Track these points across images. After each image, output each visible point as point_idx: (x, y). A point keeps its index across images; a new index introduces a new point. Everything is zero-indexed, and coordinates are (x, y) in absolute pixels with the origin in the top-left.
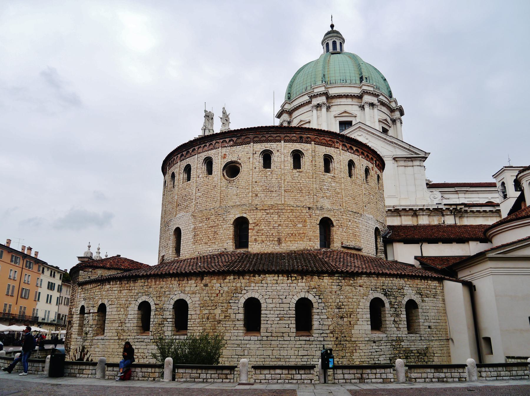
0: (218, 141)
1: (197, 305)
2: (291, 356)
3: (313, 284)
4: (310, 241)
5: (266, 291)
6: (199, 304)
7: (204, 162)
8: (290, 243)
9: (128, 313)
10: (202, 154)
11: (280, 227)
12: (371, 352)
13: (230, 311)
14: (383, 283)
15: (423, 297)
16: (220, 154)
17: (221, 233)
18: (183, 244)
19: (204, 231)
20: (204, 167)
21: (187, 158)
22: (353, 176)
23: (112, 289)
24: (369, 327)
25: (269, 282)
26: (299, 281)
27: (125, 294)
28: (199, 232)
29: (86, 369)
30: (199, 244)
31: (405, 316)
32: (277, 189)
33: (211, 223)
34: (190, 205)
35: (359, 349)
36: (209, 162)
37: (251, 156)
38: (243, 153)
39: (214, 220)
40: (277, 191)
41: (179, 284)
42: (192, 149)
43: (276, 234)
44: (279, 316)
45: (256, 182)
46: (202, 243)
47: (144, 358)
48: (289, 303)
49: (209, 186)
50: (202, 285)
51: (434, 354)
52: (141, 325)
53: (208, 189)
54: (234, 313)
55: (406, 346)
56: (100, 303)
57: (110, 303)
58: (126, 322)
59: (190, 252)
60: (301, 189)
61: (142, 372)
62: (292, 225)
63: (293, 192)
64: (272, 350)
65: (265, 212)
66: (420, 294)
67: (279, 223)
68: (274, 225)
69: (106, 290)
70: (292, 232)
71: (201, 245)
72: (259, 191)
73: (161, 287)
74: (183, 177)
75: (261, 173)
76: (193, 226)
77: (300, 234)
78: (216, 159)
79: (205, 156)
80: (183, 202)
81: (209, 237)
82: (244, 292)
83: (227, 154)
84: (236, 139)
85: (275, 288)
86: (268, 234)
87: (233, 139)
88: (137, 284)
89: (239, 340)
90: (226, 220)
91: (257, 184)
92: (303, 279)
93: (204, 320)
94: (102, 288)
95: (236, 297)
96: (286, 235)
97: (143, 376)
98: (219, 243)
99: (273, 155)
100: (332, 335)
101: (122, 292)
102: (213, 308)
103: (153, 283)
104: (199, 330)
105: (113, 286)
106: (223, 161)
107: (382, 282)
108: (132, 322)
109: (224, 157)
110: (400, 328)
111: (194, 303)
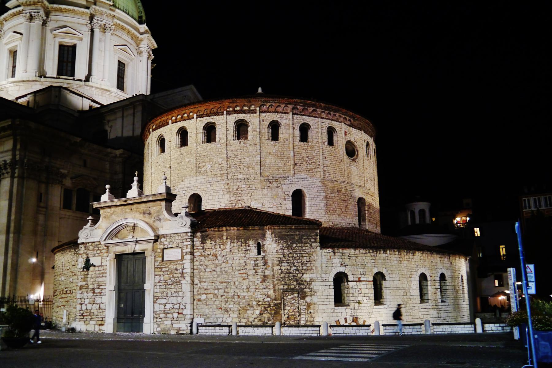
0: (341, 115)
10: (325, 120)
19: (336, 203)
27: (405, 265)
28: (331, 202)
30: (333, 215)
33: (342, 196)
38: (357, 137)
42: (312, 109)
46: (336, 214)
49: (336, 158)
57: (390, 272)
58: (411, 291)
73: (432, 262)
76: (324, 194)
80: (304, 163)
88: (415, 257)
103: (427, 258)
105: (391, 256)
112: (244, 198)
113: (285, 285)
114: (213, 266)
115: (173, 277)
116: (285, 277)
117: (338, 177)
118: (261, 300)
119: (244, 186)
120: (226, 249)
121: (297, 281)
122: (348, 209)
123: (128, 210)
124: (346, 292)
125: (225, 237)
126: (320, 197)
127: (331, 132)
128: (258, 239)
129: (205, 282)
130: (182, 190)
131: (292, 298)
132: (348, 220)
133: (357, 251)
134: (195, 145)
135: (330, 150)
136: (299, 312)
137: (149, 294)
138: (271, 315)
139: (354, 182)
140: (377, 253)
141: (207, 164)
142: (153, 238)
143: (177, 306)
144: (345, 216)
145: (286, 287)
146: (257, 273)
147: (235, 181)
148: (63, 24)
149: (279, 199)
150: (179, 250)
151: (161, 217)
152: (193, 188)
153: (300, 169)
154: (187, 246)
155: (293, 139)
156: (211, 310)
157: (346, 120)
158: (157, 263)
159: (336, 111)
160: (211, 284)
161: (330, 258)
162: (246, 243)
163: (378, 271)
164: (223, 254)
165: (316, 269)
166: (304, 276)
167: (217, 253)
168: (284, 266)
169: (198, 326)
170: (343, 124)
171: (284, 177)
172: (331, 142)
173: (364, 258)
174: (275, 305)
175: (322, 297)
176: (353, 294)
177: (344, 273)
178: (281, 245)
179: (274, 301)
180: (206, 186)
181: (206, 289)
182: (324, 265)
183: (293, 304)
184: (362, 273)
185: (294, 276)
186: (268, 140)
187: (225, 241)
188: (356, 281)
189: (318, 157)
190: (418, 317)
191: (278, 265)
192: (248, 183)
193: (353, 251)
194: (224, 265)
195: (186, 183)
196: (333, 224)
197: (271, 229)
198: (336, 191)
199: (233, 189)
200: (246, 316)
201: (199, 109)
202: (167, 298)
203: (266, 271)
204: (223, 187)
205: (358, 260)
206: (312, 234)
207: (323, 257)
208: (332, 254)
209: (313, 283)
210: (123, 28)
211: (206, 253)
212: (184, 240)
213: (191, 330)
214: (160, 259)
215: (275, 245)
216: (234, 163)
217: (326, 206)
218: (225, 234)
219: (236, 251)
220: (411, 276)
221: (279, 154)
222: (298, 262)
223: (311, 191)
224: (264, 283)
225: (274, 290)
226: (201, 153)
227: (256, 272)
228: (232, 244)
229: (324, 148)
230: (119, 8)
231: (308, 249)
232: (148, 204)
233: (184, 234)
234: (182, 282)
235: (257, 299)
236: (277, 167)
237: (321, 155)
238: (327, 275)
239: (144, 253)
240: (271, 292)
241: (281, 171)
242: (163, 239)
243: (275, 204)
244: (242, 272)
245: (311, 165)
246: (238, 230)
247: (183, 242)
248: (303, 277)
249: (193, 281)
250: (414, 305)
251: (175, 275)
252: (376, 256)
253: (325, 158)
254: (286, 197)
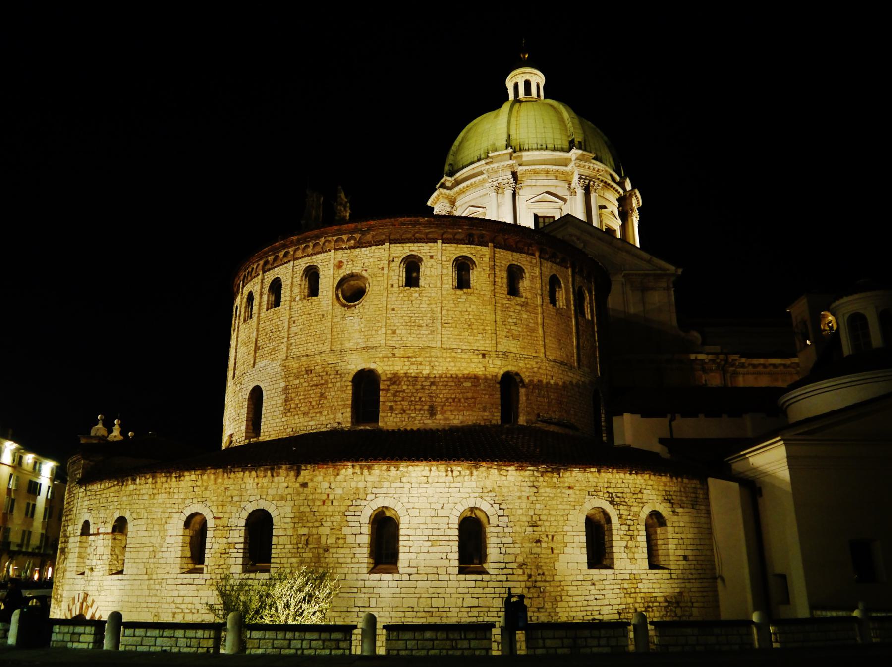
0: (330, 238)
1: (289, 520)
2: (450, 607)
3: (489, 484)
4: (484, 411)
5: (408, 495)
6: (291, 518)
7: (304, 274)
8: (450, 414)
9: (165, 534)
10: (300, 261)
11: (434, 388)
12: (588, 600)
13: (346, 531)
14: (607, 482)
15: (674, 506)
17: (331, 397)
18: (267, 415)
19: (302, 393)
20: (305, 284)
21: (276, 267)
22: (557, 303)
23: (138, 493)
24: (585, 558)
25: (414, 480)
26: (466, 478)
27: (160, 501)
28: (293, 395)
29: (84, 633)
30: (294, 416)
31: (644, 539)
32: (429, 321)
33: (315, 379)
34: (279, 348)
35: (567, 595)
36: (312, 276)
37: (386, 266)
38: (371, 260)
39: (321, 374)
40: (430, 325)
41: (257, 484)
42: (283, 253)
43: (427, 399)
44: (431, 538)
45: (393, 310)
46: (299, 413)
47: (193, 613)
48: (449, 517)
49: (313, 315)
50: (298, 485)
51: (692, 603)
52: (189, 554)
53: (311, 321)
54: (353, 534)
55: (646, 590)
56: (117, 516)
57: (135, 516)
58: (163, 549)
60: (469, 323)
61: (187, 638)
62: (453, 384)
63: (456, 327)
64: (418, 598)
65: (408, 361)
66: (670, 502)
67: (432, 380)
68: (424, 384)
69: (128, 493)
70: (453, 396)
71: (296, 417)
72: (399, 325)
73: (226, 488)
74: (268, 301)
75: (402, 295)
76: (283, 385)
77: (467, 398)
78: (325, 269)
79: (306, 264)
80: (267, 342)
81: (311, 402)
82: (369, 497)
83: (344, 261)
84: (359, 235)
85: (424, 490)
86: (413, 398)
87: (355, 235)
88: (182, 484)
89: (362, 580)
90: (341, 375)
91: (394, 312)
92: (472, 476)
93: (300, 546)
94: (122, 490)
95: (356, 505)
96: (443, 400)
97: (188, 645)
98: (328, 414)
99: (423, 264)
100: (521, 572)
101: (156, 497)
102: (317, 524)
103: (212, 482)
104: (291, 563)
106: (337, 273)
107: (606, 480)
108: (172, 549)
109: (340, 265)
110: (636, 559)
111: (283, 515)
117: (311, 347)
122: (326, 398)
132: (323, 418)
135: (304, 306)
139: (349, 345)
140: (123, 485)
144: (316, 413)
148: (467, 205)
157: (343, 241)
159: (318, 237)
190: (170, 600)
196: (292, 431)
198: (304, 372)
210: (536, 172)
217: (284, 404)
230: (529, 149)
250: (167, 577)
253: (294, 322)
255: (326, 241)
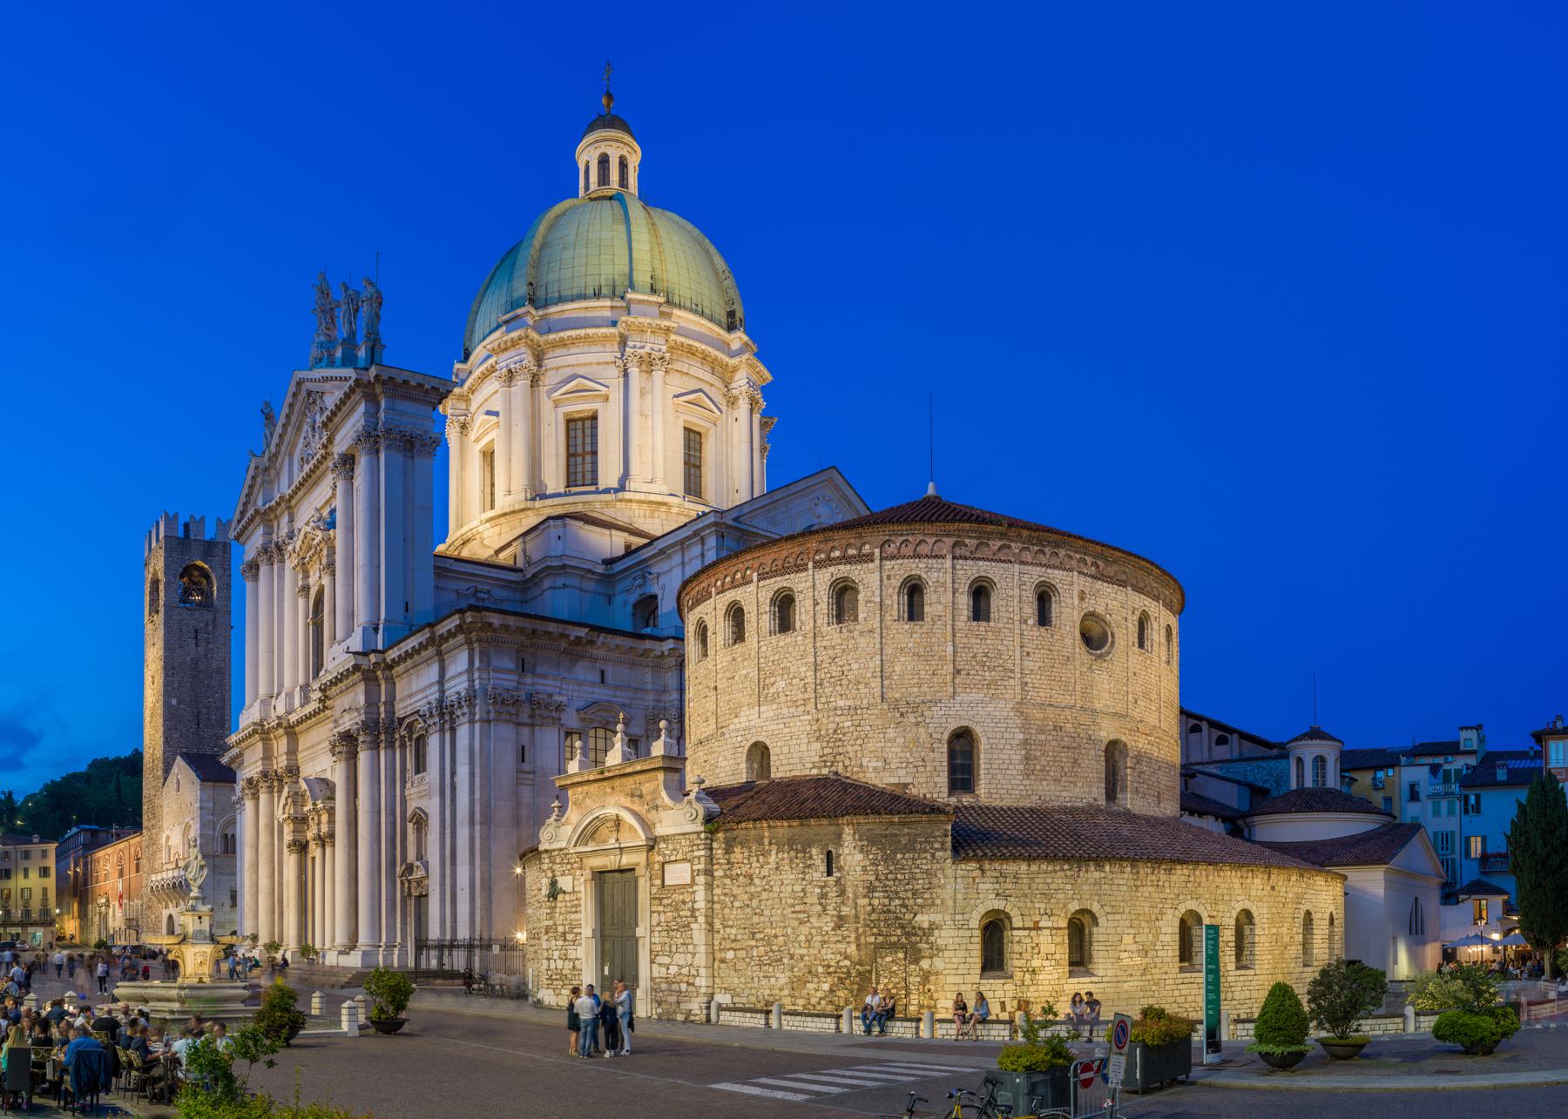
0: (1072, 554)
16: (1076, 586)
27: (1147, 894)
28: (1038, 754)
34: (1005, 683)
49: (1055, 653)
57: (1108, 909)
59: (1017, 792)
71: (1044, 783)
76: (1021, 736)
79: (1040, 576)
80: (978, 668)
101: (1140, 889)
112: (849, 748)
113: (880, 935)
114: (746, 897)
115: (679, 916)
116: (879, 919)
117: (1056, 696)
118: (833, 963)
119: (849, 724)
120: (768, 863)
121: (902, 927)
123: (609, 790)
124: (1009, 950)
125: (766, 841)
126: (1013, 742)
127: (1044, 598)
128: (827, 845)
129: (731, 927)
130: (736, 734)
131: (893, 961)
133: (1034, 867)
134: (756, 640)
135: (1040, 636)
136: (906, 988)
137: (644, 946)
138: (852, 992)
141: (779, 678)
142: (644, 843)
143: (685, 971)
145: (880, 939)
146: (825, 910)
147: (832, 713)
149: (920, 749)
150: (688, 865)
151: (658, 802)
152: (754, 730)
153: (968, 681)
154: (699, 858)
155: (953, 616)
156: (743, 980)
157: (1086, 564)
158: (654, 890)
160: (743, 931)
161: (974, 881)
162: (805, 852)
163: (1082, 907)
164: (762, 874)
165: (942, 903)
166: (919, 918)
167: (752, 871)
168: (879, 898)
169: (720, 1008)
170: (1076, 573)
171: (931, 701)
172: (1044, 619)
173: (1050, 881)
174: (860, 973)
175: (954, 960)
176: (1021, 954)
177: (1004, 911)
178: (871, 857)
179: (857, 967)
180: (775, 727)
181: (734, 941)
182: (959, 896)
183: (895, 972)
184: (1042, 911)
185: (897, 918)
186: (899, 620)
187: (767, 847)
188: (1028, 929)
189: (1010, 653)
191: (865, 896)
192: (855, 717)
193: (1024, 867)
194: (765, 895)
195: (742, 721)
197: (853, 824)
199: (827, 730)
200: (804, 993)
201: (762, 560)
202: (670, 954)
203: (843, 908)
204: (808, 728)
205: (1034, 886)
206: (937, 833)
207: (959, 880)
208: (978, 872)
209: (936, 933)
211: (734, 872)
212: (695, 847)
213: (708, 1015)
214: (658, 882)
215: (860, 857)
216: (828, 676)
218: (766, 834)
219: (787, 868)
220: (1160, 917)
221: (922, 650)
222: (905, 891)
223: (991, 729)
224: (839, 932)
225: (858, 945)
226: (768, 654)
227: (825, 910)
228: (780, 855)
229: (1025, 633)
231: (927, 864)
232: (637, 777)
233: (695, 836)
234: (692, 926)
235: (826, 963)
236: (916, 681)
237: (1018, 648)
238: (966, 916)
239: (634, 869)
240: (852, 949)
241: (925, 688)
242: (662, 845)
243: (911, 760)
244: (798, 908)
245: (993, 673)
246: (789, 826)
247: (693, 851)
248: (917, 919)
249: (711, 925)
251: (681, 913)
252: (1078, 876)
253: (1028, 654)
254: (935, 746)
255: (1067, 555)
